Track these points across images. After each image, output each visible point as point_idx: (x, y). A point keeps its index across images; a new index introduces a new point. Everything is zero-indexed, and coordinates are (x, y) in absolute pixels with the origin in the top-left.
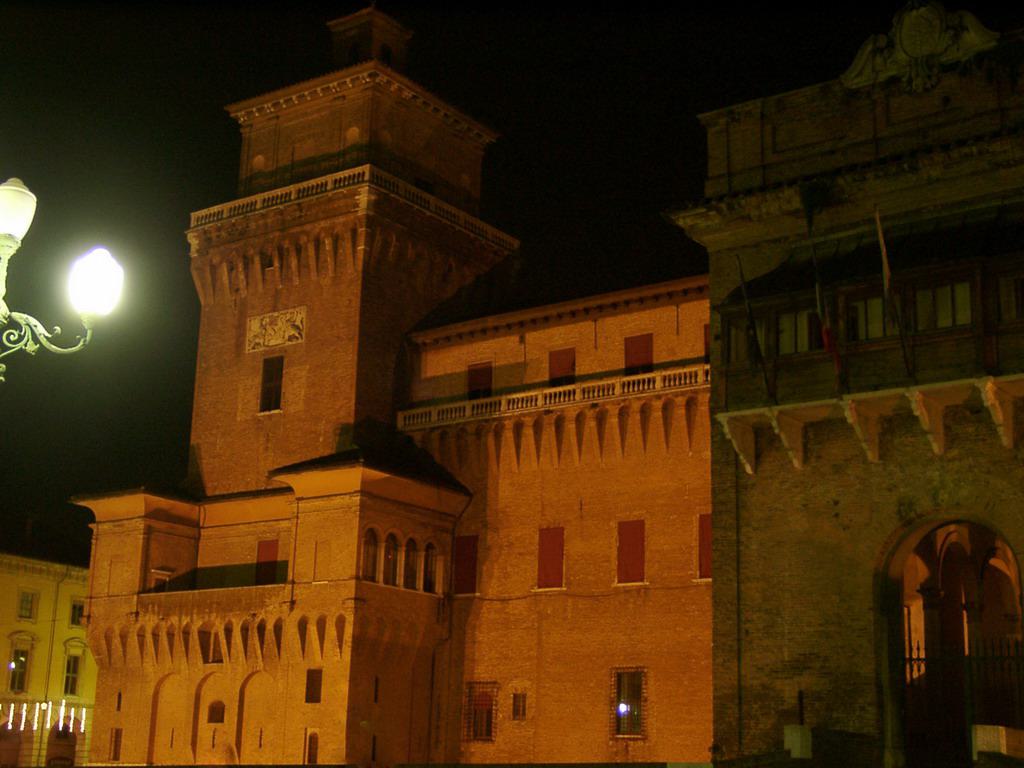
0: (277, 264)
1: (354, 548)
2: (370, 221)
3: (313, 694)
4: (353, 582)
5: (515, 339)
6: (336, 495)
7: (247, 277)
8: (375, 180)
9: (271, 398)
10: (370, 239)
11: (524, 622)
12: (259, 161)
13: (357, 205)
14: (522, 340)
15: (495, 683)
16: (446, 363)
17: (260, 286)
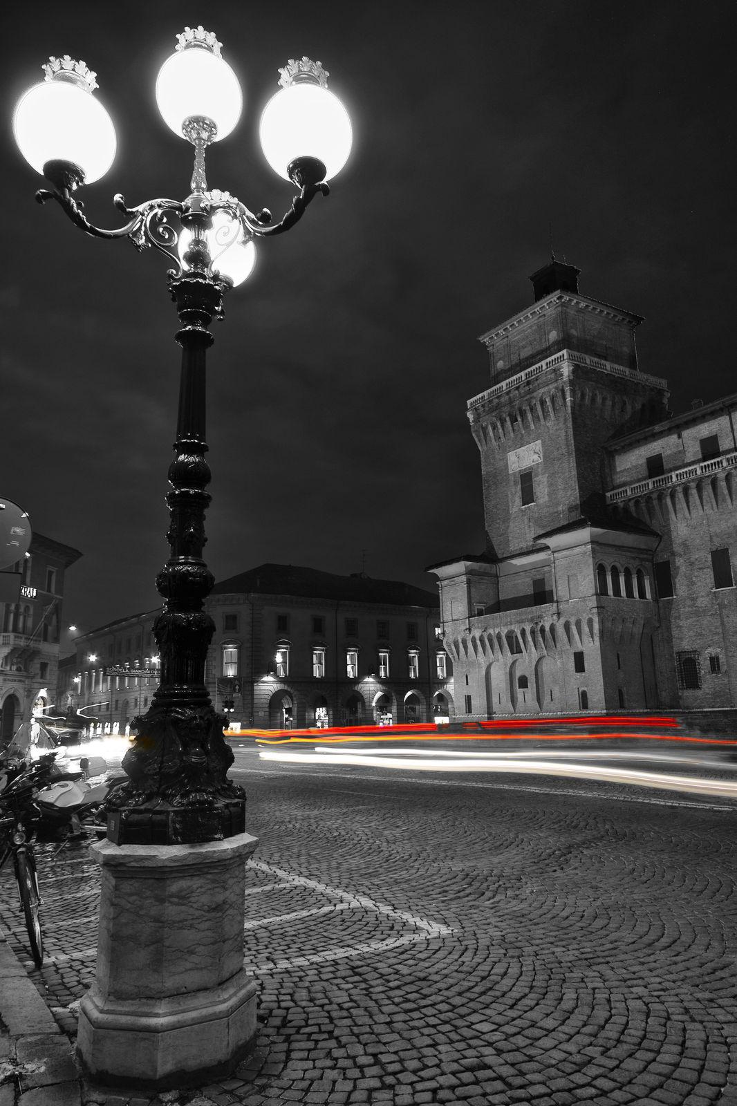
0: (519, 419)
1: (592, 577)
2: (571, 383)
3: (580, 667)
4: (595, 597)
5: (675, 436)
6: (575, 547)
7: (503, 430)
8: (571, 358)
9: (528, 497)
10: (573, 392)
11: (710, 611)
12: (500, 364)
13: (562, 375)
14: (680, 436)
15: (695, 651)
16: (631, 462)
17: (512, 434)
